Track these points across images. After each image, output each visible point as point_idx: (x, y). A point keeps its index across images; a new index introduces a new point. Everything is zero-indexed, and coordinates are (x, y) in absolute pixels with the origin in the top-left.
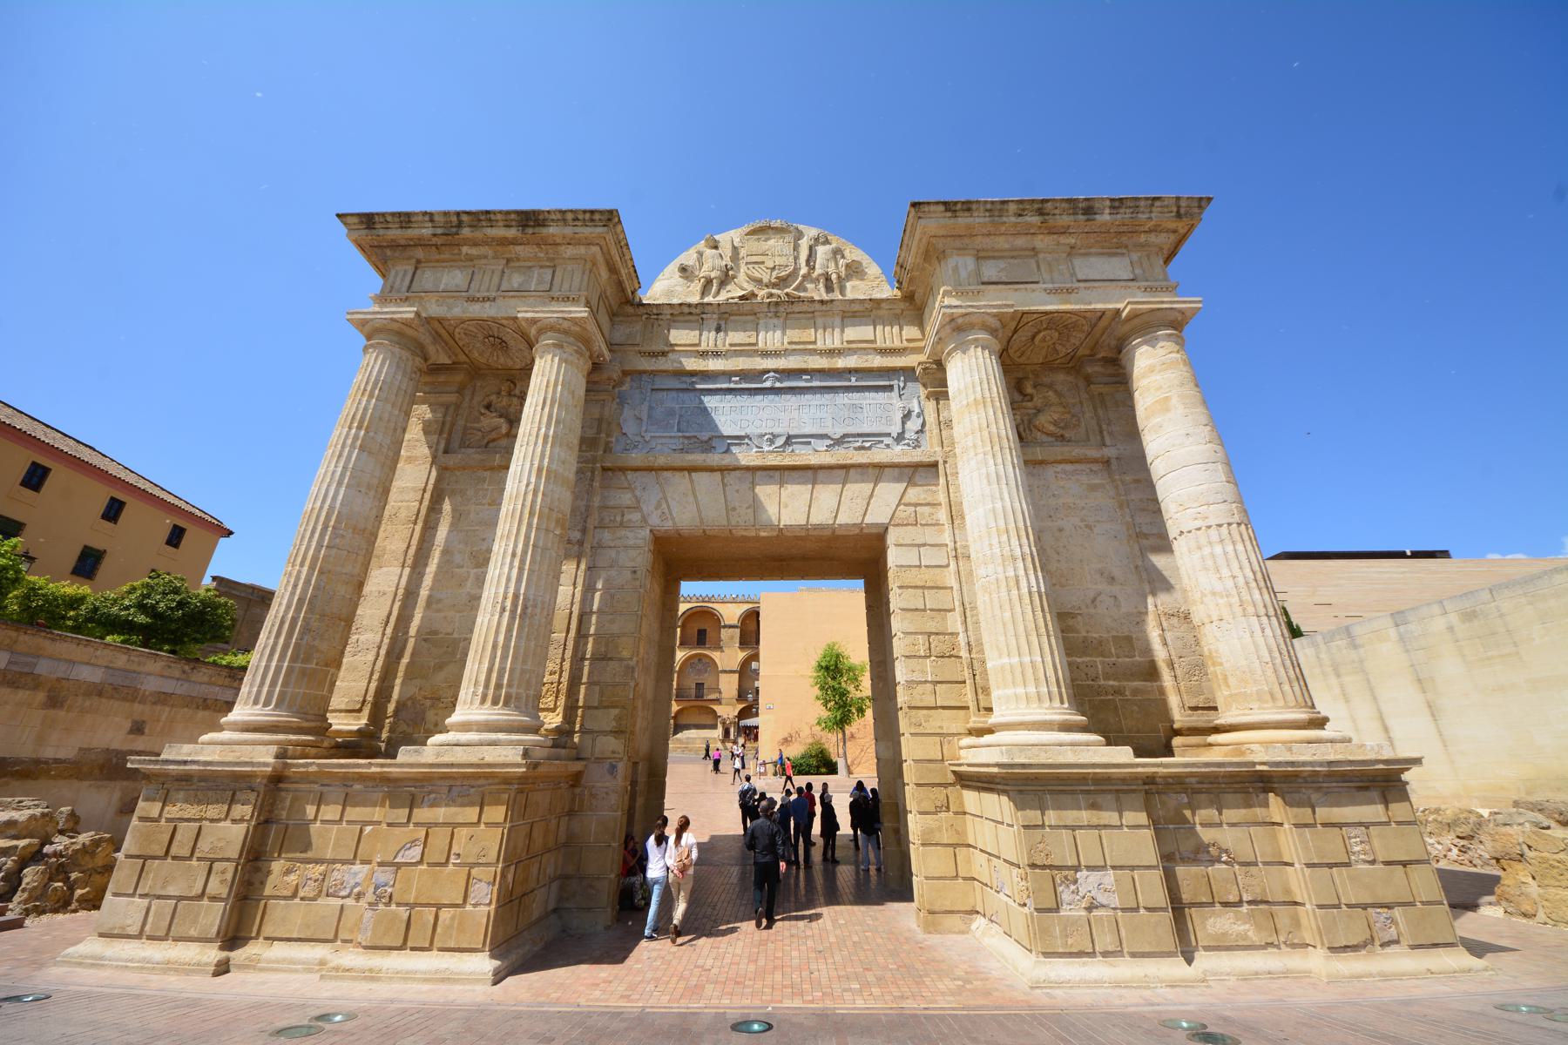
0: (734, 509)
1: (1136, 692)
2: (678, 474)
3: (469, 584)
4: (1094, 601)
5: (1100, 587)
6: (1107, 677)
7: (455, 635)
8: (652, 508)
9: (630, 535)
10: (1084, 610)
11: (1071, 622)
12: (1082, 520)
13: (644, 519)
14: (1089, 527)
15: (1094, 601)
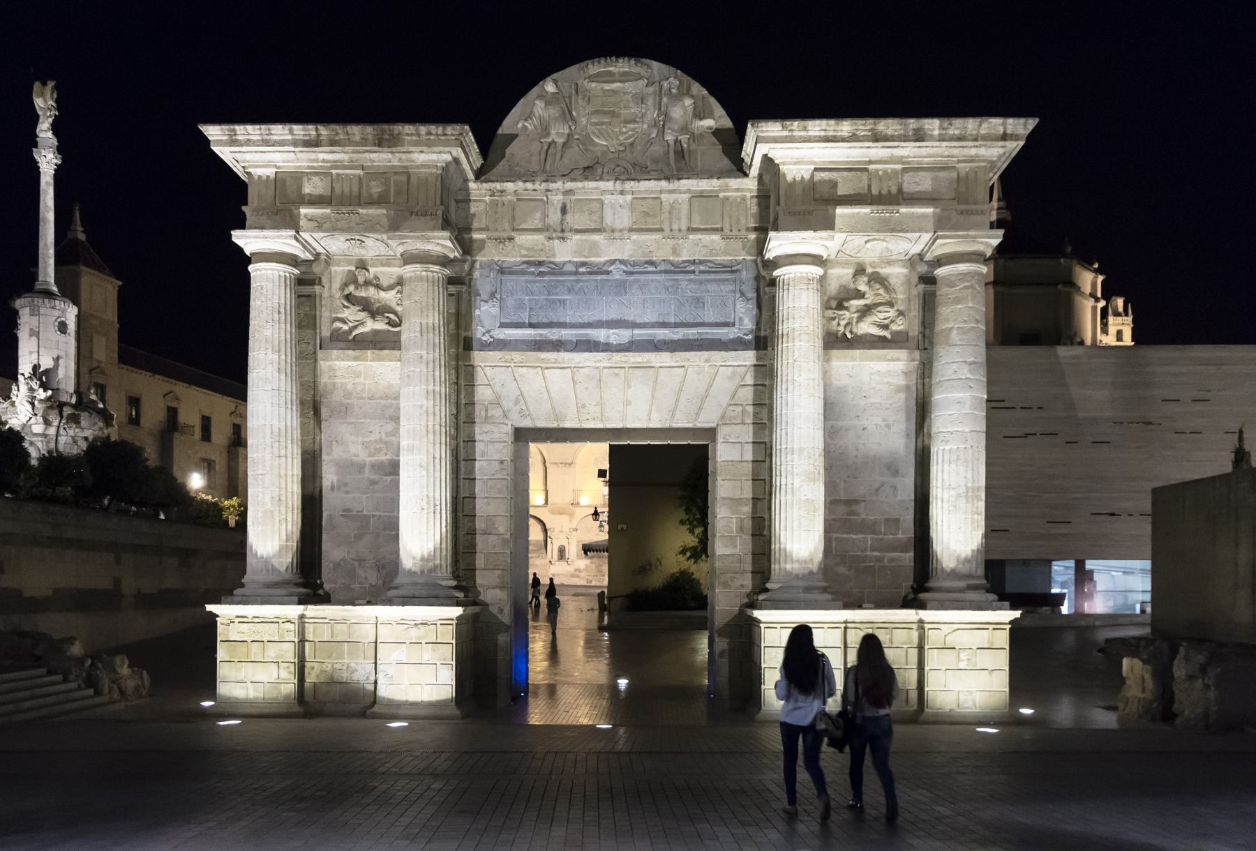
0: (584, 406)
1: (892, 560)
2: (531, 371)
3: (367, 471)
4: (877, 490)
5: (885, 479)
6: (872, 550)
7: (365, 513)
8: (511, 404)
9: (495, 429)
10: (868, 498)
11: (854, 507)
12: (884, 420)
13: (505, 416)
14: (888, 426)
15: (877, 490)
